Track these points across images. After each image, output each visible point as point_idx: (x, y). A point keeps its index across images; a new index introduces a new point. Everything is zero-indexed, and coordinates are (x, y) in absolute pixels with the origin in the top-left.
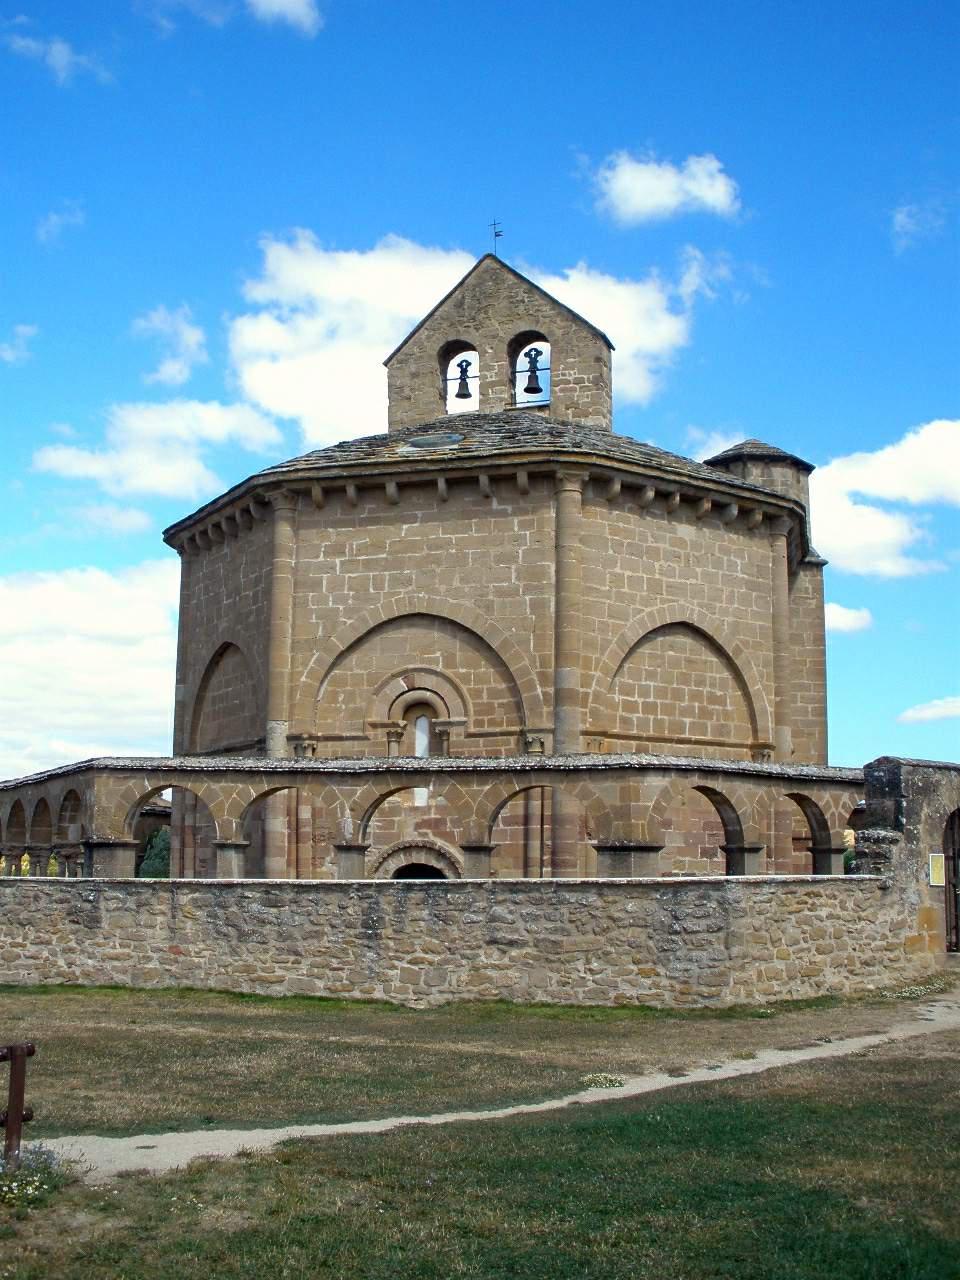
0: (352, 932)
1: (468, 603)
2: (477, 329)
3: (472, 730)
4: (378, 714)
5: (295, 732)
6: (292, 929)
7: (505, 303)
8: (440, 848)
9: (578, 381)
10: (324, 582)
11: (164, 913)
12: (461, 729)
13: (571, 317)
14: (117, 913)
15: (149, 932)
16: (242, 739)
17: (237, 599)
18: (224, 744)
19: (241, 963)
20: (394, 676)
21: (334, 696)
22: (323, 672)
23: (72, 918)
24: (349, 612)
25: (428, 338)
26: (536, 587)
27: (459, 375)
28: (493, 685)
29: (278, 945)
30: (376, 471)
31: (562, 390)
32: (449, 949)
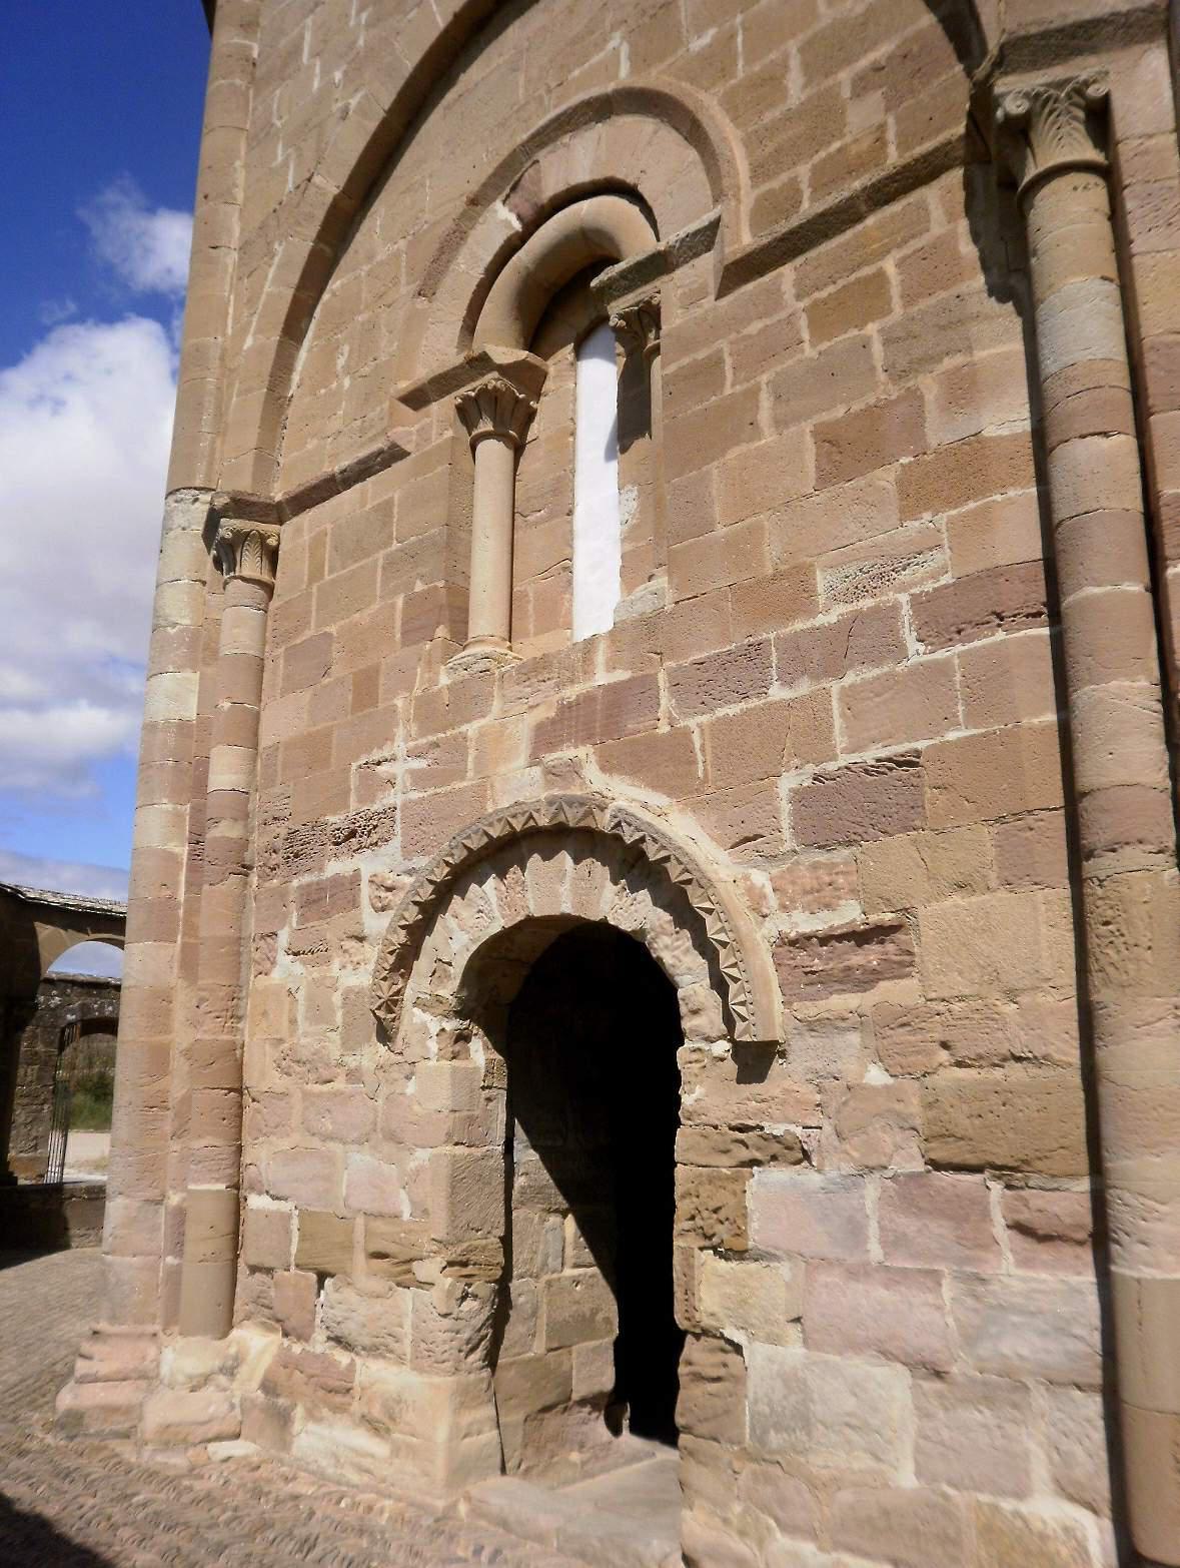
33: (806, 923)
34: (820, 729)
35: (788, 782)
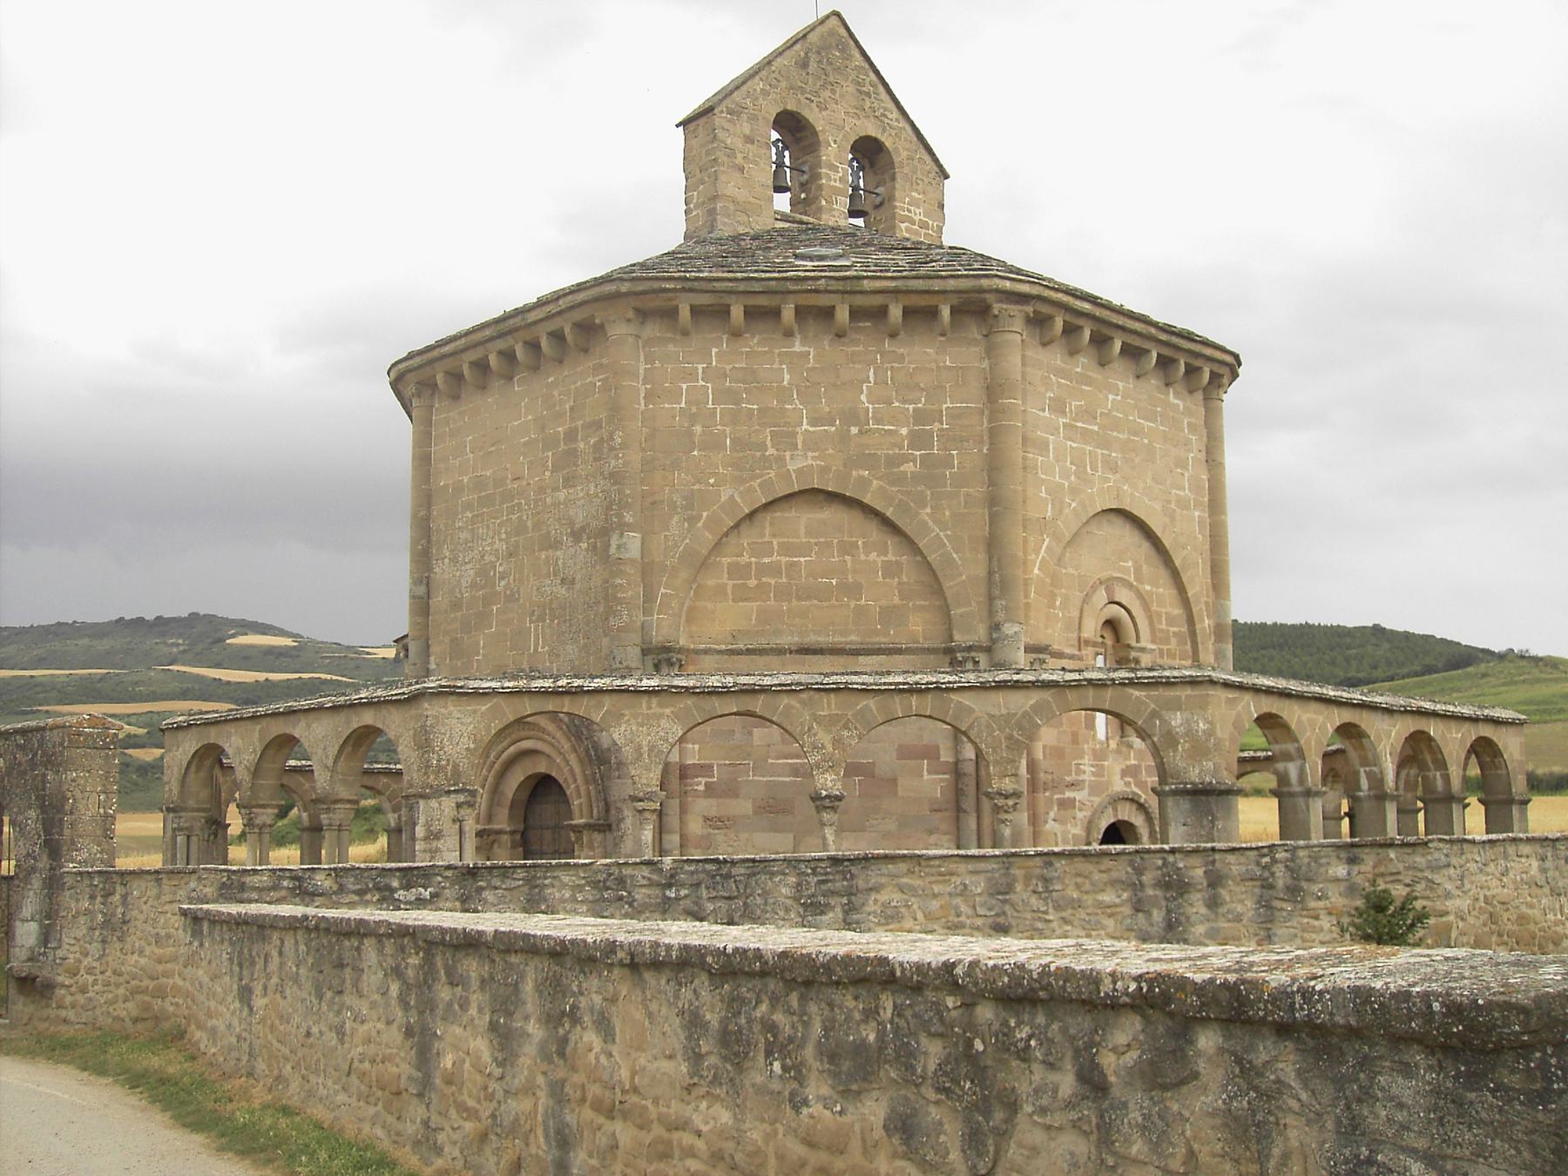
1: (1158, 506)
7: (851, 89)
16: (853, 638)
17: (854, 430)
18: (788, 640)
25: (765, 93)
28: (1169, 610)
31: (907, 230)
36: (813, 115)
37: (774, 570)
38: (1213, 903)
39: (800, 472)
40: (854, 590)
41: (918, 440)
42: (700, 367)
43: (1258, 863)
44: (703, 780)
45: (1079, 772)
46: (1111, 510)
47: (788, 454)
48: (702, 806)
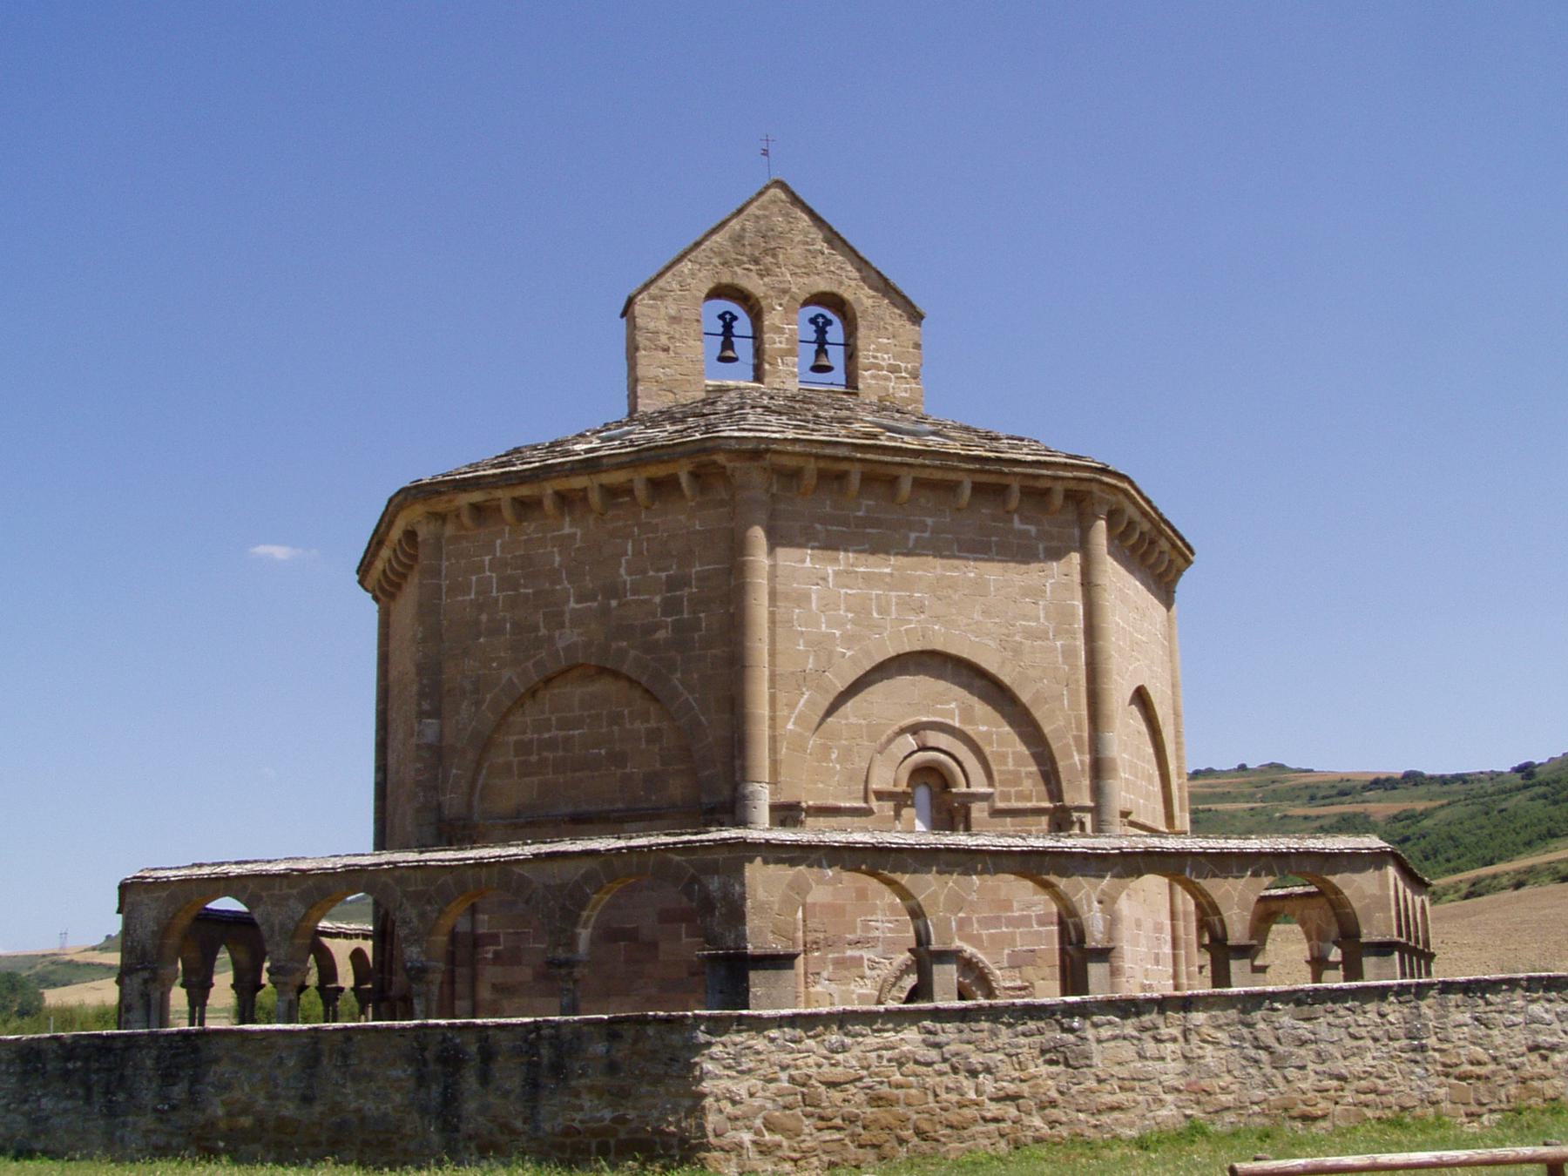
0: (1396, 1044)
2: (762, 276)
3: (1000, 805)
4: (883, 779)
5: (783, 798)
6: (1330, 1048)
8: (973, 956)
9: (894, 369)
10: (814, 597)
11: (1174, 1040)
12: (984, 805)
13: (881, 285)
14: (1112, 1044)
15: (1159, 1065)
16: (620, 805)
19: (1277, 1096)
20: (903, 731)
21: (826, 749)
22: (817, 720)
23: (1048, 1056)
24: (849, 640)
25: (693, 275)
26: (1068, 632)
27: (721, 330)
29: (1319, 1068)
30: (898, 459)
32: (1495, 1059)
33: (1008, 984)
34: (1014, 940)
35: (1006, 951)
36: (753, 284)
37: (551, 744)
38: (485, 1078)
39: (568, 649)
40: (619, 759)
41: (671, 606)
42: (487, 558)
43: (526, 1040)
44: (492, 948)
45: (866, 927)
46: (922, 652)
47: (557, 633)
48: (491, 973)
